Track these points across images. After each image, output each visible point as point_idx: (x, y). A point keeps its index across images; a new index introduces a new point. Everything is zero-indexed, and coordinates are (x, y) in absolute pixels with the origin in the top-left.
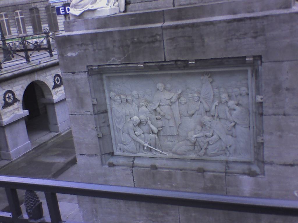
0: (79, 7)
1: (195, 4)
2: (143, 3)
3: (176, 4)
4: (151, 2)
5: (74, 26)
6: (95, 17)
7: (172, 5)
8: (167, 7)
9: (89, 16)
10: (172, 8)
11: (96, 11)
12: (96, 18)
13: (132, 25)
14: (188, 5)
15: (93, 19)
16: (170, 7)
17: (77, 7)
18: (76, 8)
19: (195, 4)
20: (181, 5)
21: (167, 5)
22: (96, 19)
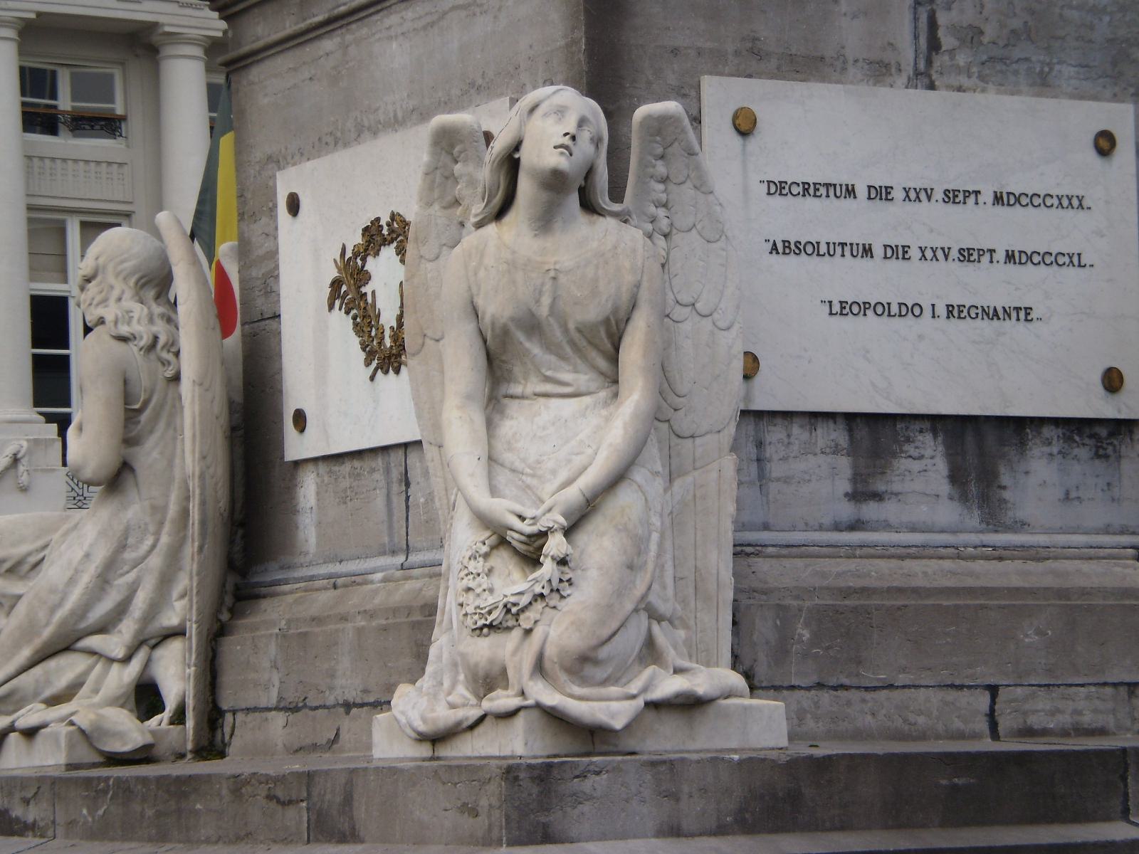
0: (600, 673)
1: (1102, 732)
2: (826, 697)
3: (1004, 724)
4: (868, 696)
5: (578, 798)
6: (735, 751)
7: (982, 725)
8: (961, 736)
9: (667, 739)
10: (988, 745)
11: (711, 710)
12: (736, 757)
13: (953, 819)
14: (1065, 733)
15: (716, 761)
16: (975, 736)
17: (589, 670)
18: (584, 681)
19: (1102, 732)
20: (1028, 732)
21: (957, 724)
22: (741, 762)
